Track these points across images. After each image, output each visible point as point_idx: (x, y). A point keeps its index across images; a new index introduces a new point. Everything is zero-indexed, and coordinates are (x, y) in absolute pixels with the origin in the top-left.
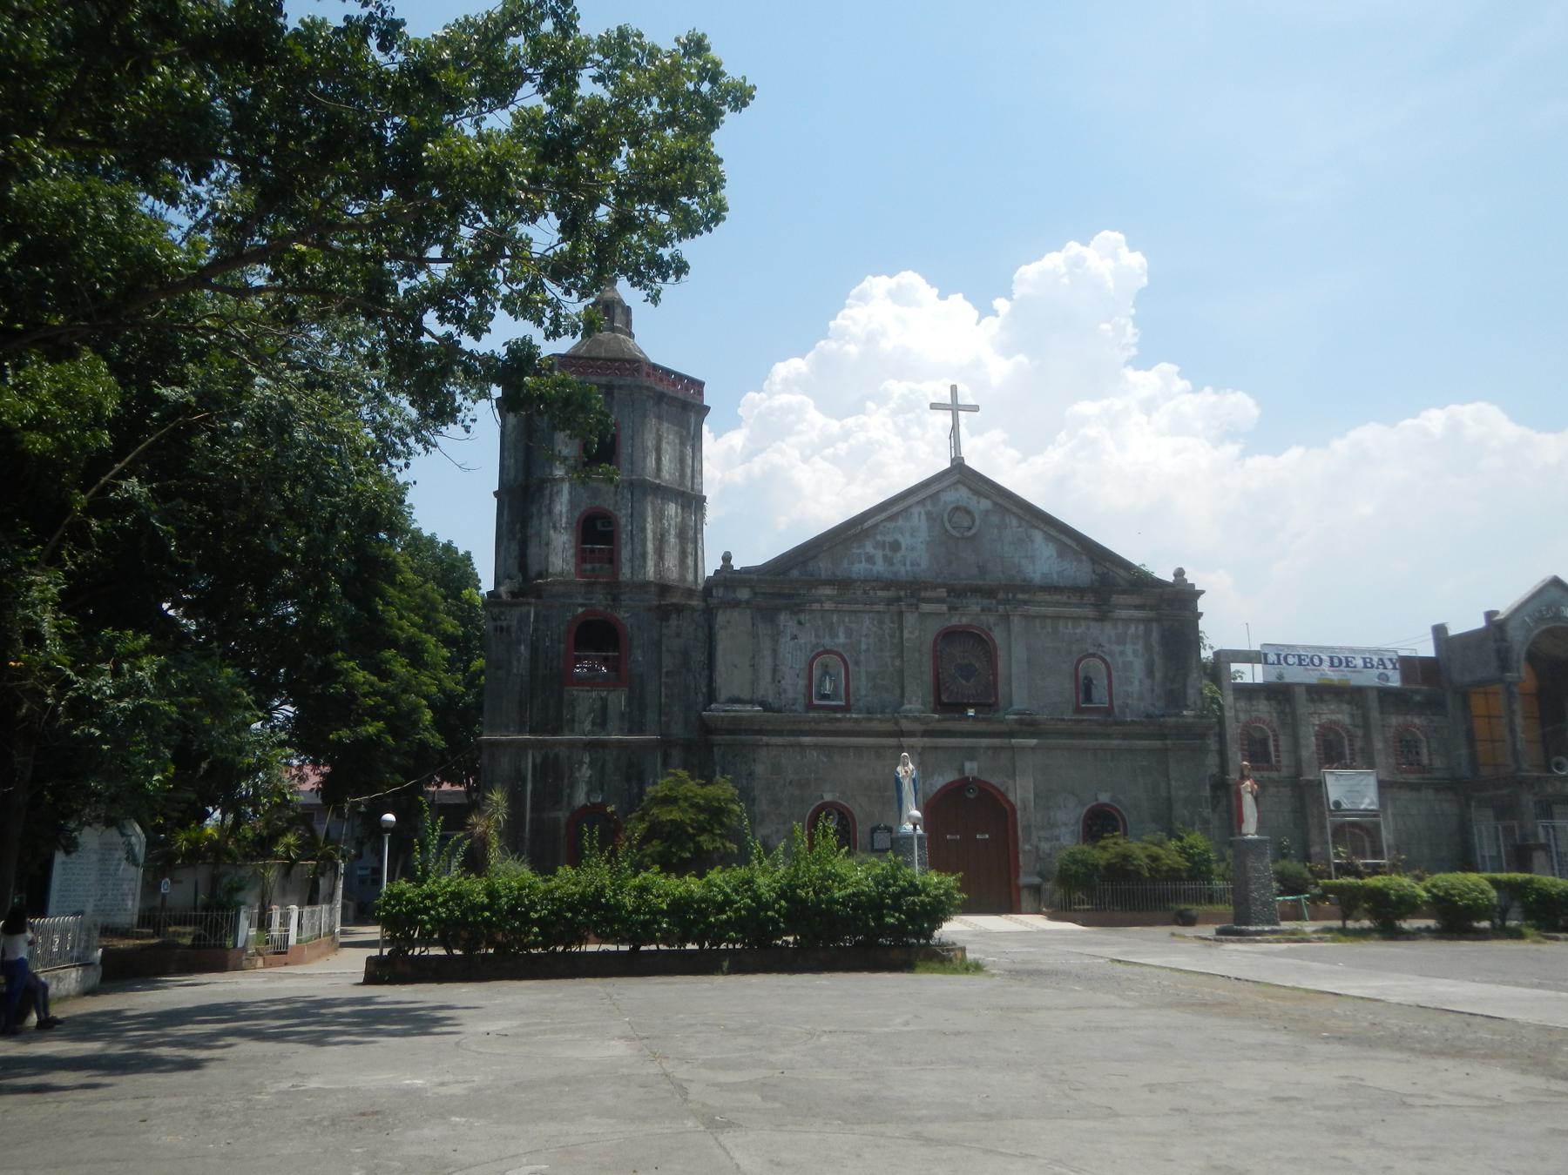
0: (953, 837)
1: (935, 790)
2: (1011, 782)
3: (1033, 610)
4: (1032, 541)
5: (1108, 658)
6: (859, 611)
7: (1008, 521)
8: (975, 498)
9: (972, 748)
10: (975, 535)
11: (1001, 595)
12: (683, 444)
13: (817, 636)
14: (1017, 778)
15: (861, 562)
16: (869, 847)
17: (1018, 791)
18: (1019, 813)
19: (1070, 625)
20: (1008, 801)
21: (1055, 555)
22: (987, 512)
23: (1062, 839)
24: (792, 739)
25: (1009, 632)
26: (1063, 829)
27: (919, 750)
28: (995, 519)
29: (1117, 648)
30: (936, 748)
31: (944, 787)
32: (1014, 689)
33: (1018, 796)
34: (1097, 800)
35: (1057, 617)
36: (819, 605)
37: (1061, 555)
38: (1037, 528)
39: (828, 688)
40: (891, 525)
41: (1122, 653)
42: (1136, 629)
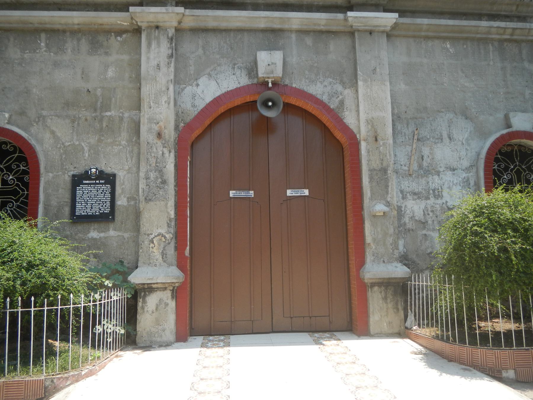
0: (243, 194)
1: (201, 105)
2: (348, 93)
9: (273, 31)
14: (360, 83)
16: (67, 210)
17: (361, 108)
18: (363, 146)
20: (346, 129)
23: (445, 194)
26: (448, 177)
27: (171, 32)
30: (206, 30)
31: (216, 101)
33: (363, 116)
34: (509, 126)
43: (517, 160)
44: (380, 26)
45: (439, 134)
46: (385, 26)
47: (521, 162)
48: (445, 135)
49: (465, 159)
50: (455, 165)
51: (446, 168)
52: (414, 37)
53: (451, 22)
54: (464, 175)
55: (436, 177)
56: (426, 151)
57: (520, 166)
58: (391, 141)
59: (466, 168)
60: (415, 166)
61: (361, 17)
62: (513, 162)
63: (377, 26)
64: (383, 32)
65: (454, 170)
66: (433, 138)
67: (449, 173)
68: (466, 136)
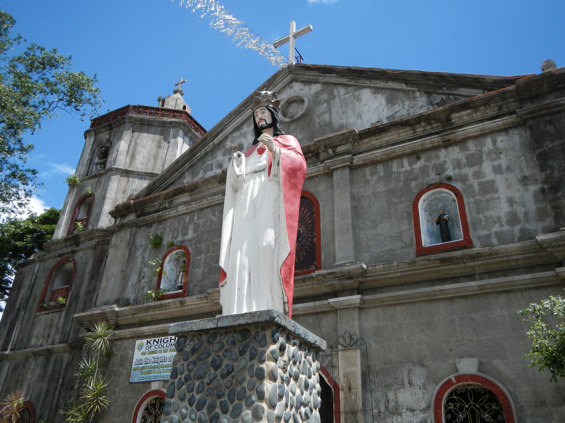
3: (357, 160)
4: (359, 99)
5: (458, 185)
6: (206, 208)
7: (336, 93)
8: (307, 87)
10: (304, 115)
11: (322, 155)
12: (159, 146)
13: (172, 238)
15: (212, 170)
18: (341, 393)
19: (406, 162)
21: (384, 102)
22: (317, 94)
24: (135, 329)
25: (332, 187)
28: (325, 96)
29: (469, 171)
32: (337, 243)
34: (457, 371)
35: (387, 160)
36: (175, 211)
37: (391, 101)
38: (365, 87)
39: (181, 279)
40: (236, 134)
41: (478, 175)
42: (494, 142)
43: (471, 400)
44: (352, 304)
45: (401, 381)
46: (356, 304)
47: (475, 401)
48: (406, 382)
49: (423, 401)
50: (414, 406)
51: (407, 409)
52: (382, 306)
53: (402, 293)
54: (422, 416)
55: (399, 417)
56: (391, 395)
57: (474, 405)
58: (360, 390)
59: (424, 409)
60: (382, 409)
61: (337, 302)
62: (468, 402)
63: (350, 305)
64: (356, 307)
65: (413, 411)
66: (397, 384)
67: (410, 413)
68: (423, 381)
